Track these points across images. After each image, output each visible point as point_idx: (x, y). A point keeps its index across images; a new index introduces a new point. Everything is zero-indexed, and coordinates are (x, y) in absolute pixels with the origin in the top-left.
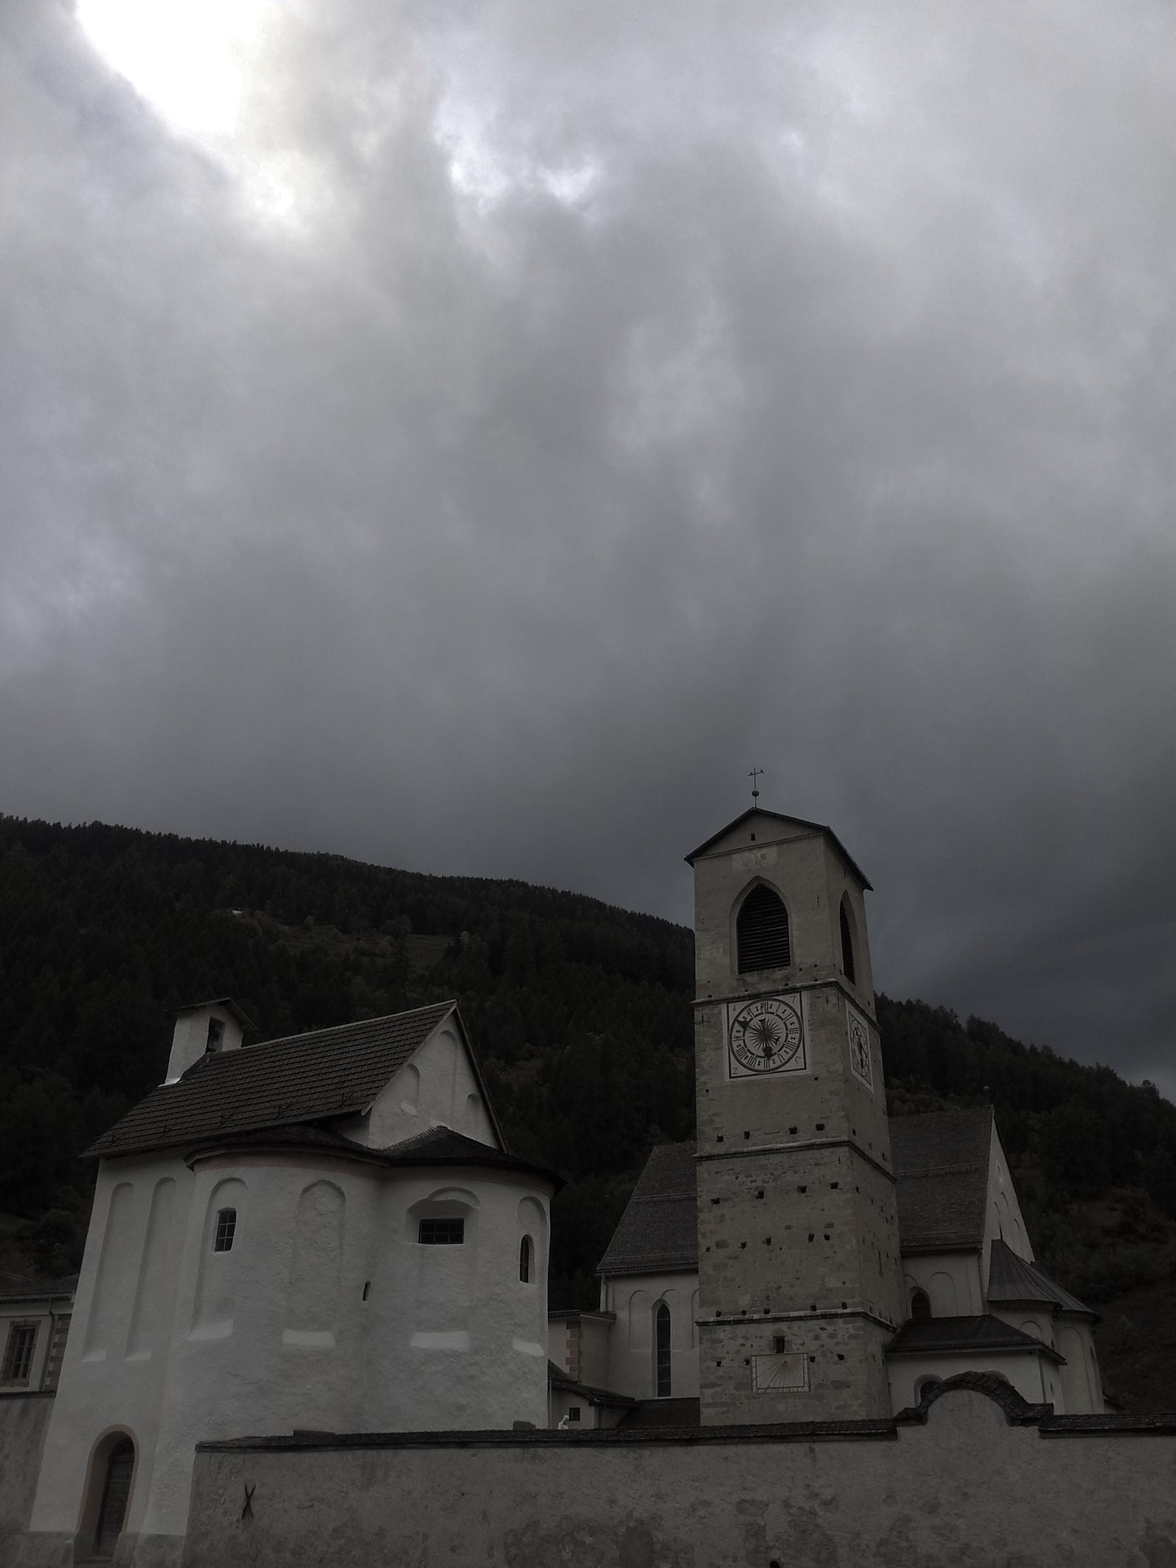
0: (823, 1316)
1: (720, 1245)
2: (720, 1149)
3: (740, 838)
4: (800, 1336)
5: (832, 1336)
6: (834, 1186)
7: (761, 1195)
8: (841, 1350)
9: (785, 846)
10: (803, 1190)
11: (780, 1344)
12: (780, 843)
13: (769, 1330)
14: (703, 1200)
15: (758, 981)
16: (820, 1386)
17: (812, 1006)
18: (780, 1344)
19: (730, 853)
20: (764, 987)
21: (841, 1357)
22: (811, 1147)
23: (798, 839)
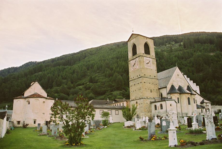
0: (140, 99)
1: (132, 91)
2: (131, 80)
3: (132, 38)
4: (138, 101)
5: (141, 101)
6: (141, 82)
7: (135, 85)
8: (142, 103)
9: (136, 38)
10: (138, 83)
11: (137, 103)
12: (135, 38)
13: (136, 101)
14: (130, 86)
15: (135, 57)
16: (140, 107)
17: (139, 59)
18: (137, 103)
19: (131, 40)
20: (134, 58)
21: (142, 104)
22: (139, 78)
23: (137, 36)
